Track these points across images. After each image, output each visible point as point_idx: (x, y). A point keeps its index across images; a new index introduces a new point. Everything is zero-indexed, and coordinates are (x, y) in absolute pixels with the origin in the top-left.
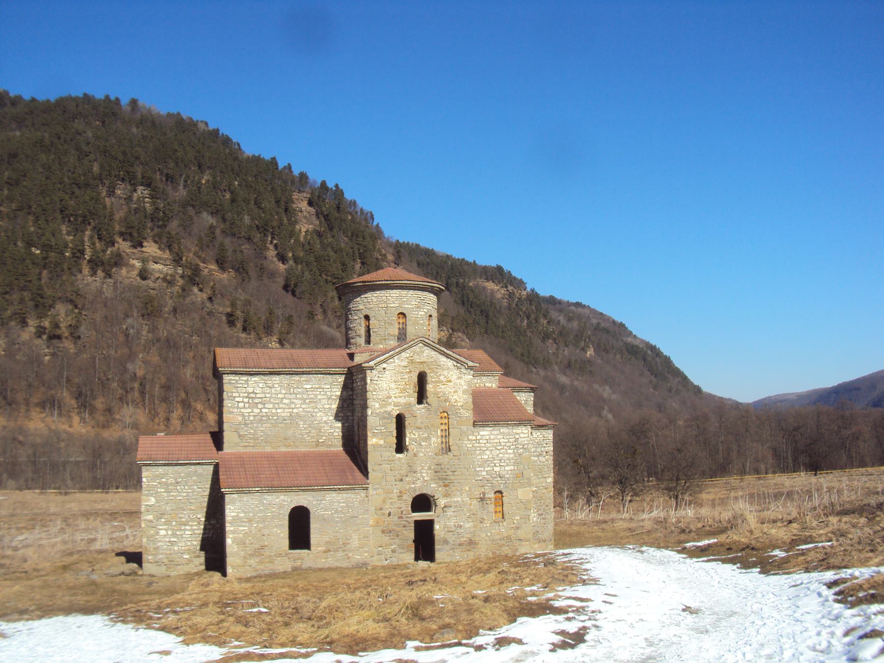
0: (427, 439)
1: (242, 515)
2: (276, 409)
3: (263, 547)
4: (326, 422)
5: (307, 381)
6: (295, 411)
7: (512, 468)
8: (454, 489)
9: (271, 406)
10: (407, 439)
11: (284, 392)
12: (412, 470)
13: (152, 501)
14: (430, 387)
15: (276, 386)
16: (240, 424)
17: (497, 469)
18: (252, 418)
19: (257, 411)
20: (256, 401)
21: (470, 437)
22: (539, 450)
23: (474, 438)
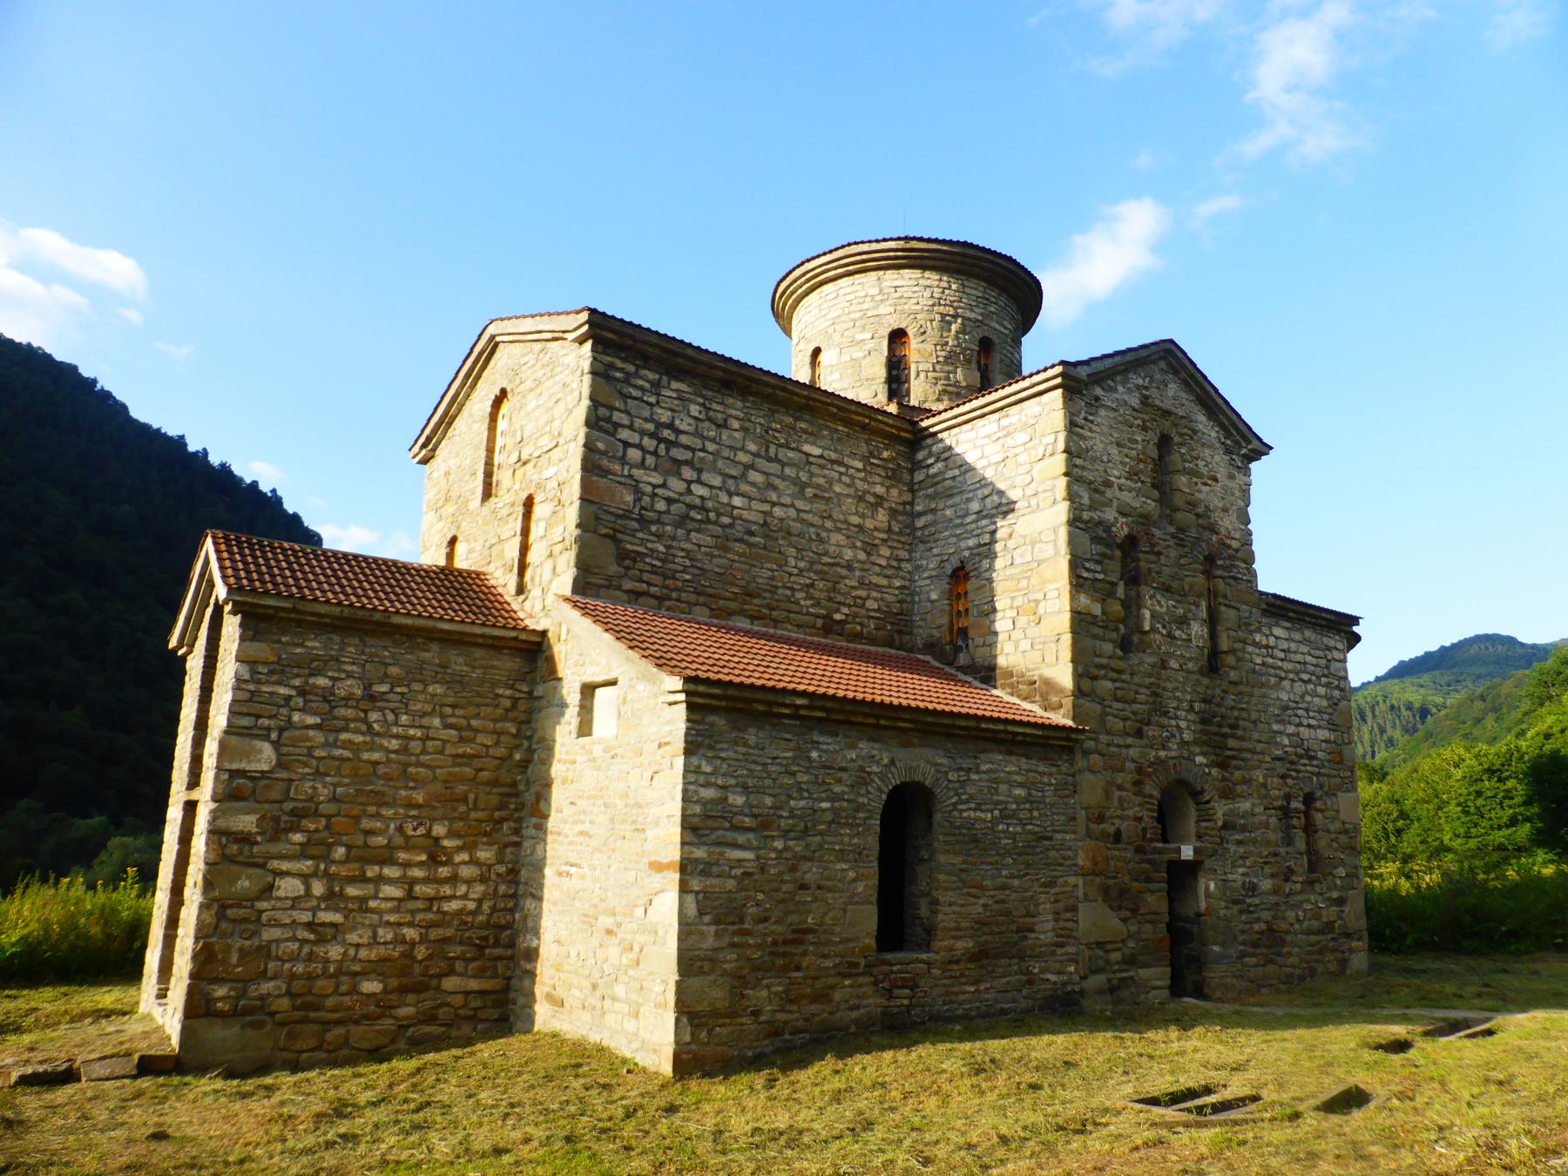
0: (1183, 622)
1: (738, 800)
2: (730, 494)
3: (800, 935)
4: (849, 567)
5: (814, 436)
6: (778, 511)
9: (717, 481)
10: (1147, 614)
11: (752, 447)
13: (264, 756)
15: (736, 424)
16: (626, 515)
18: (661, 505)
19: (676, 485)
20: (677, 453)
21: (1258, 637)
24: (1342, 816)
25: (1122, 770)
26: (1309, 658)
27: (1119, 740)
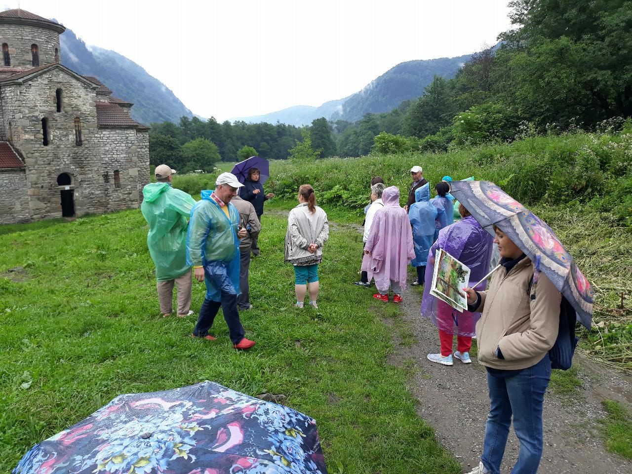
0: (67, 135)
7: (125, 155)
8: (87, 169)
10: (52, 136)
12: (56, 156)
14: (65, 100)
17: (115, 156)
21: (96, 135)
22: (141, 144)
23: (99, 136)
24: (130, 174)
25: (44, 172)
26: (117, 138)
27: (43, 166)
